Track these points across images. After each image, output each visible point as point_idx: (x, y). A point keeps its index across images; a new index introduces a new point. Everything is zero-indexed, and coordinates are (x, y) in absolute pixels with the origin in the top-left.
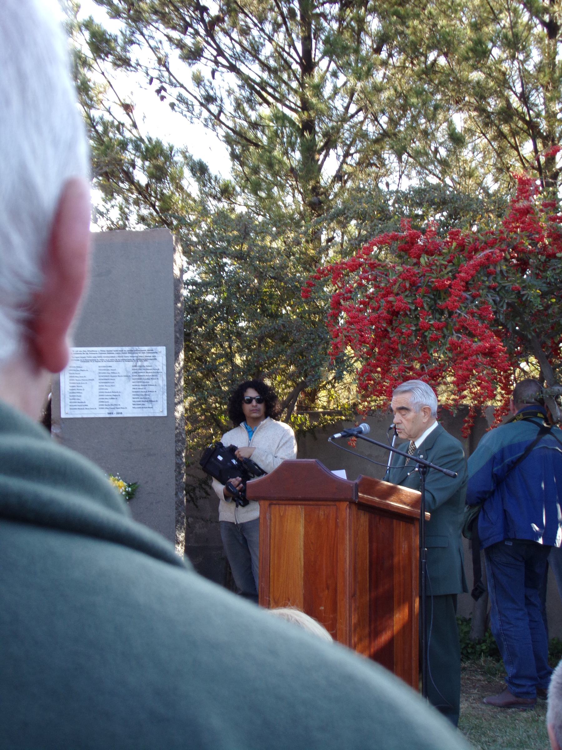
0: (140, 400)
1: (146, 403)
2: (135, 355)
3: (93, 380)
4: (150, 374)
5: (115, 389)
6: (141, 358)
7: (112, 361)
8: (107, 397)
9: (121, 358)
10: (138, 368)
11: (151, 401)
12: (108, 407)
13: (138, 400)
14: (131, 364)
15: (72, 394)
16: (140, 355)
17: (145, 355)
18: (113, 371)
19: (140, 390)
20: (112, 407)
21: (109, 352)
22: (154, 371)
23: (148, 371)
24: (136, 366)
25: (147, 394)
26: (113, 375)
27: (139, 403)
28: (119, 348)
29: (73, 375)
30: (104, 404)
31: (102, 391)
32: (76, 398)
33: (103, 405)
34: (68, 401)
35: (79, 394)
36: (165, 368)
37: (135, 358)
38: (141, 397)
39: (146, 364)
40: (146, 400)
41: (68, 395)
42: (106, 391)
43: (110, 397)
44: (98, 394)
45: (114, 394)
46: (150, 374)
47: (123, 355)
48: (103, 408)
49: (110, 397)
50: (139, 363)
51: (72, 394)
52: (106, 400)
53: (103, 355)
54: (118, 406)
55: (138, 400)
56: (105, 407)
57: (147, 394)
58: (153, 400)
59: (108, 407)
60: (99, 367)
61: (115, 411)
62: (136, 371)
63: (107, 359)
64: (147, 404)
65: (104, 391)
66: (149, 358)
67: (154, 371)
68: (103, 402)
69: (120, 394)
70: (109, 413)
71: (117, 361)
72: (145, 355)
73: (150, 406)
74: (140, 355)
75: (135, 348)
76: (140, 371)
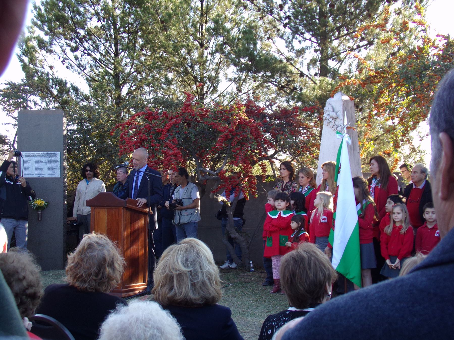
5: (41, 167)
7: (40, 157)
14: (47, 158)
28: (43, 153)
39: (53, 158)
61: (41, 175)
64: (53, 173)
75: (49, 153)
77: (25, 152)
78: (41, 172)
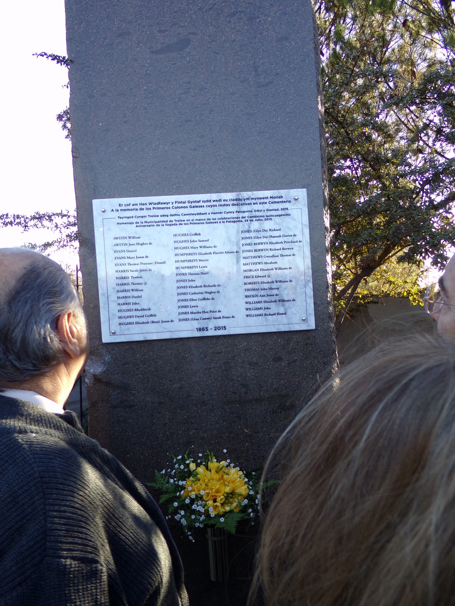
0: (260, 299)
1: (272, 305)
2: (245, 208)
3: (164, 263)
4: (278, 246)
6: (258, 214)
7: (199, 222)
8: (194, 297)
9: (219, 216)
10: (252, 235)
11: (283, 301)
12: (197, 316)
13: (256, 299)
15: (121, 294)
16: (256, 207)
17: (267, 206)
18: (203, 244)
19: (259, 280)
20: (206, 316)
21: (194, 204)
22: (286, 239)
23: (274, 240)
24: (249, 231)
25: (274, 285)
26: (204, 251)
27: (259, 305)
28: (214, 196)
29: (122, 255)
30: (189, 310)
31: (183, 284)
32: (131, 300)
33: (186, 313)
34: (114, 307)
35: (136, 294)
36: (307, 231)
37: (246, 214)
38: (262, 293)
39: (268, 225)
40: (273, 299)
41: (113, 297)
42: (192, 284)
43: (201, 296)
44: (176, 291)
45: (209, 290)
46: (278, 246)
47: (223, 209)
48: (186, 320)
49: (201, 296)
50: (255, 225)
51: (121, 294)
52: (193, 303)
53: (181, 211)
54: (218, 315)
55: (256, 299)
56: (190, 316)
57: (274, 285)
58: (286, 299)
59: (197, 316)
60: (175, 235)
61: (211, 324)
62: (248, 241)
63: (191, 217)
64: (274, 308)
65: (188, 284)
66: (274, 213)
67: (286, 239)
68: (186, 307)
69: (220, 289)
70: (200, 330)
71: (209, 221)
72: (267, 206)
73: (282, 311)
74: (256, 207)
75: (245, 195)
76: (257, 241)
77: (116, 201)
78: (208, 305)
